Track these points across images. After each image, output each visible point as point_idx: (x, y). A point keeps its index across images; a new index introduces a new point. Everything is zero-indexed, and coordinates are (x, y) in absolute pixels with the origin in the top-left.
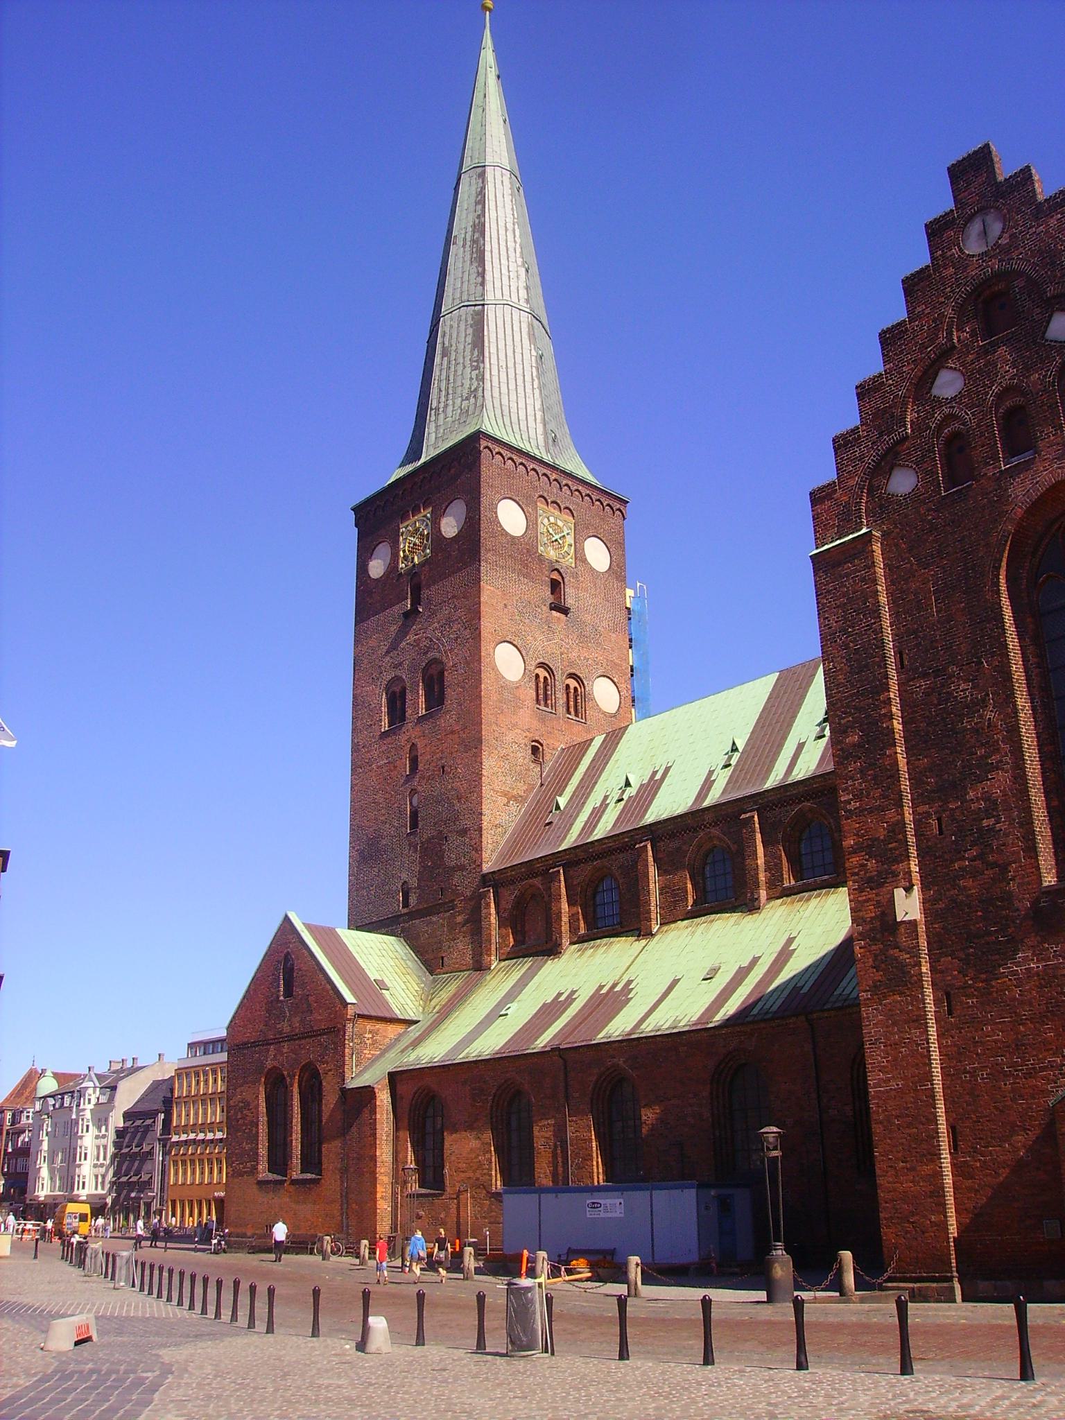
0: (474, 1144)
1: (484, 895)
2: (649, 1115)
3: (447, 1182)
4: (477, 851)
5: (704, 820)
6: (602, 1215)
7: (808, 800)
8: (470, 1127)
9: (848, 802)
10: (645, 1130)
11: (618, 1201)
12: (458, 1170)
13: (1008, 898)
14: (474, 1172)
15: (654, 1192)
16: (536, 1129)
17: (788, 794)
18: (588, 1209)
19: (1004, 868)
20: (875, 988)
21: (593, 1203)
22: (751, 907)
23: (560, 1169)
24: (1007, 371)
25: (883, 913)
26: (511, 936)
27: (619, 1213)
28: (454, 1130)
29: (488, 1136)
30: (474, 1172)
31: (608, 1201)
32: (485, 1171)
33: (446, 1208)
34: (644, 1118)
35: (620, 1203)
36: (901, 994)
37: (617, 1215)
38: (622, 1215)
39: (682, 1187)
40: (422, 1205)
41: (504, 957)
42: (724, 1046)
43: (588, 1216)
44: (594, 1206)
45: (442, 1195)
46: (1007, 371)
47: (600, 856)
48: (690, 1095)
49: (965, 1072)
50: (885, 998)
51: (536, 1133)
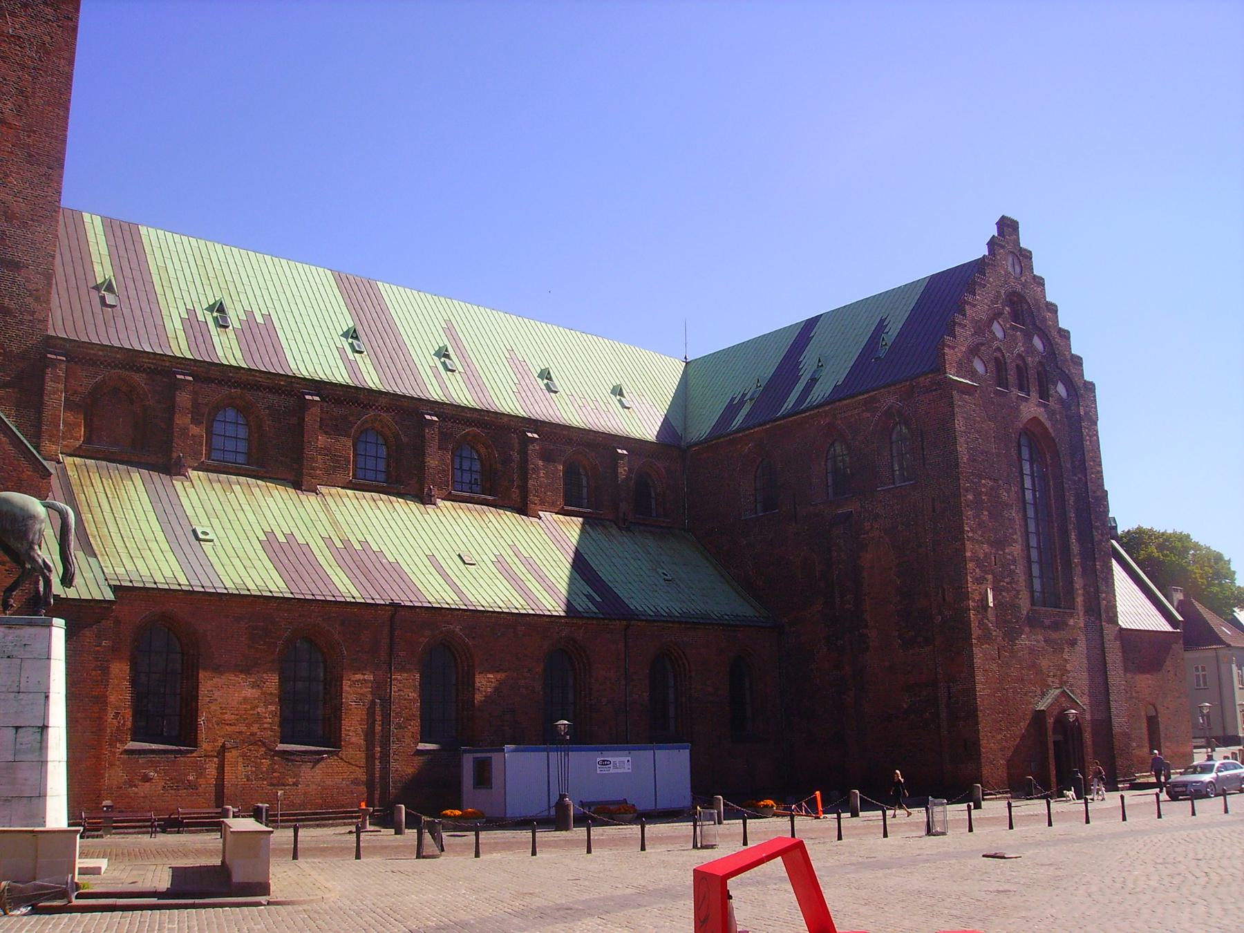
0: (250, 692)
1: (54, 363)
2: (485, 683)
3: (202, 735)
4: (37, 299)
5: (377, 402)
6: (612, 771)
7: (478, 428)
8: (245, 669)
9: (968, 531)
10: (479, 697)
11: (626, 759)
12: (221, 722)
13: (1019, 607)
14: (249, 725)
15: (550, 753)
16: (346, 685)
17: (463, 414)
18: (598, 766)
19: (1018, 592)
20: (978, 638)
21: (604, 761)
22: (424, 498)
23: (378, 728)
24: (1020, 348)
25: (982, 600)
26: (83, 429)
27: (627, 768)
28: (218, 670)
29: (272, 682)
30: (249, 725)
31: (617, 759)
32: (266, 726)
33: (201, 772)
34: (478, 685)
35: (628, 761)
36: (989, 644)
37: (626, 771)
38: (630, 771)
39: (679, 748)
40: (154, 765)
41: (69, 451)
42: (558, 633)
43: (598, 772)
44: (604, 763)
45: (192, 752)
46: (1020, 348)
47: (238, 384)
48: (526, 670)
49: (1004, 689)
50: (983, 645)
51: (345, 688)
